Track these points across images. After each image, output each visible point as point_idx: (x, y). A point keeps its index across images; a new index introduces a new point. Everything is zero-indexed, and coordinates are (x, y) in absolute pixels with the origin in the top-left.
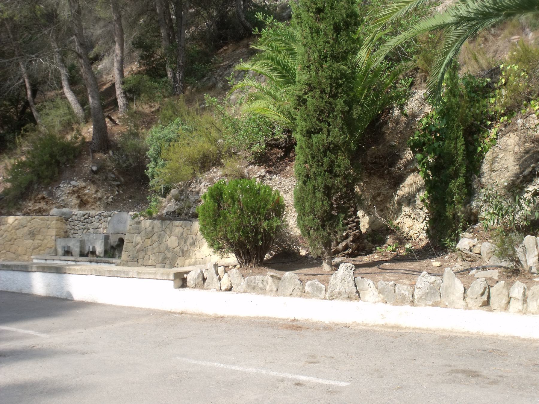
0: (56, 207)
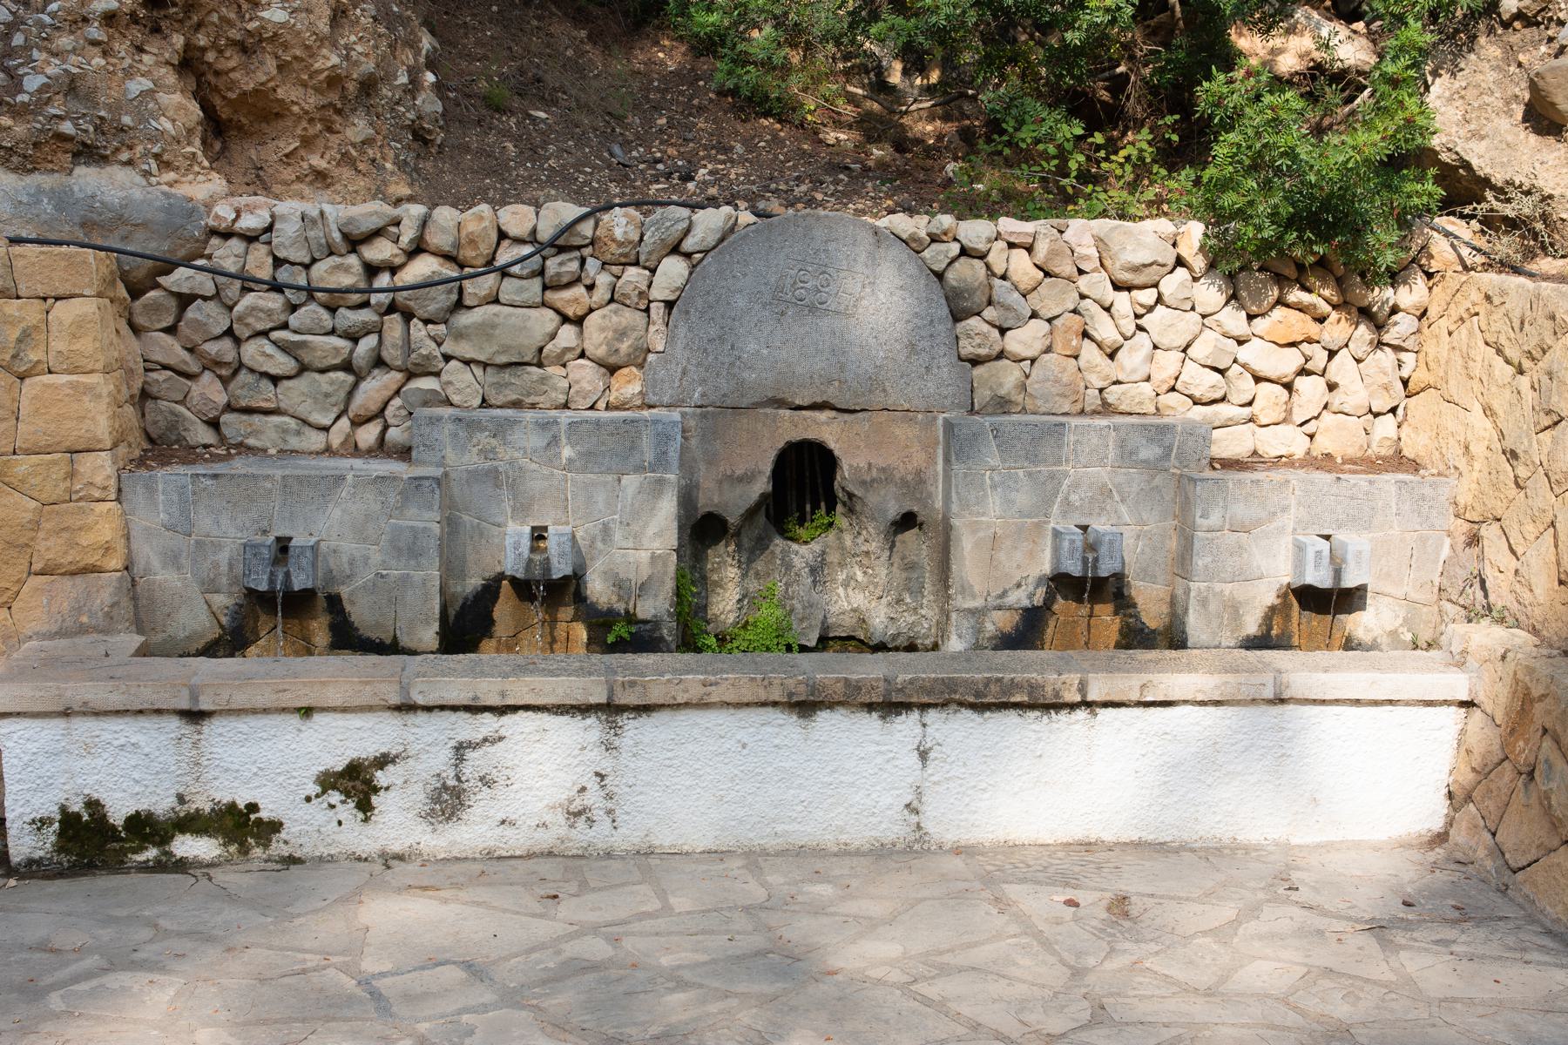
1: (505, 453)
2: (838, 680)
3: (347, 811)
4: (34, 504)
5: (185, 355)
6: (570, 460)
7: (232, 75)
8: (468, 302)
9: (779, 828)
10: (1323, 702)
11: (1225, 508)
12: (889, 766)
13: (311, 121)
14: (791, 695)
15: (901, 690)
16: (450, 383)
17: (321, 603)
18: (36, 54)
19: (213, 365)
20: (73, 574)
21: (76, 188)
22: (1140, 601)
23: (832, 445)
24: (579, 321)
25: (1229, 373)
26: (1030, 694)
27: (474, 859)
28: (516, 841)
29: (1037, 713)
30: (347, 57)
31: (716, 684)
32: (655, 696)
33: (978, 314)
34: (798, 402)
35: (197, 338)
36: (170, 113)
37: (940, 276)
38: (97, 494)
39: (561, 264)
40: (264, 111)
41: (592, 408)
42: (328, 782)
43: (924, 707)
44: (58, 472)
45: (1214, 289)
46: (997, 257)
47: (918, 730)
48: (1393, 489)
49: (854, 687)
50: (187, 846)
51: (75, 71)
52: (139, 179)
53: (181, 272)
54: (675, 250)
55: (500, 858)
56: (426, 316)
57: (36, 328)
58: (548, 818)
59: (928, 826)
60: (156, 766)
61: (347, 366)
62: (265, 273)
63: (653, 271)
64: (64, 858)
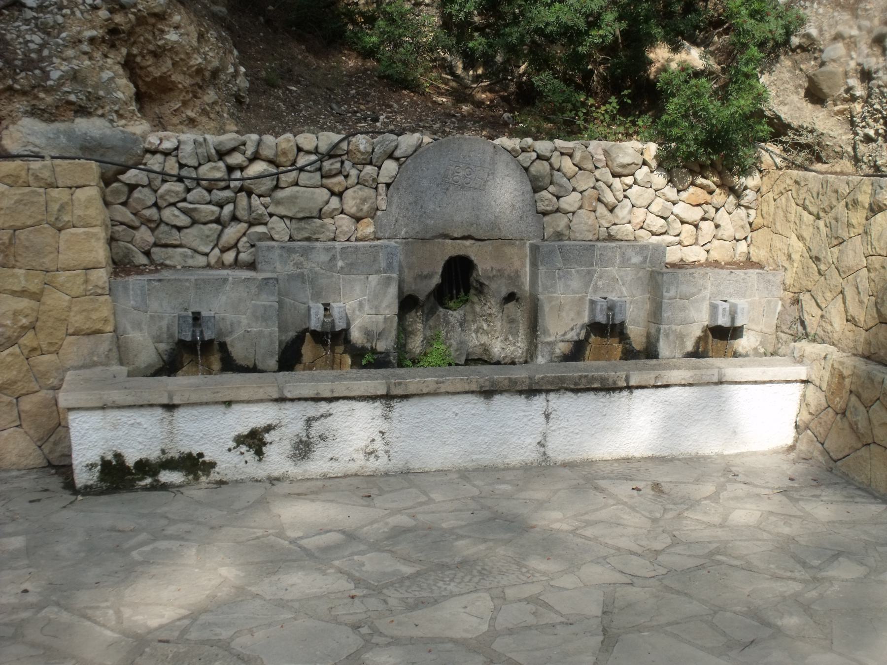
0: (34, 112)
1: (308, 265)
2: (505, 379)
3: (250, 455)
4: (68, 298)
5: (132, 216)
6: (342, 268)
7: (149, 69)
8: (282, 185)
9: (474, 457)
10: (740, 383)
11: (677, 287)
12: (529, 423)
13: (187, 92)
14: (481, 387)
15: (537, 383)
16: (273, 228)
17: (216, 347)
18: (55, 60)
19: (147, 221)
20: (88, 334)
21: (77, 130)
22: (631, 335)
23: (473, 258)
24: (340, 195)
25: (669, 219)
26: (601, 383)
27: (317, 479)
28: (336, 469)
29: (604, 393)
30: (205, 59)
31: (443, 382)
32: (412, 389)
33: (546, 189)
34: (455, 235)
35: (139, 208)
36: (122, 89)
37: (526, 169)
38: (100, 291)
39: (332, 164)
40: (164, 87)
41: (348, 240)
42: (240, 440)
43: (548, 391)
44: (80, 280)
45: (661, 177)
46: (555, 160)
47: (545, 403)
48: (756, 277)
49: (513, 382)
50: (166, 476)
51: (77, 68)
52: (107, 124)
53: (133, 172)
54: (391, 156)
55: (330, 478)
56: (260, 193)
57: (67, 203)
58: (355, 456)
59: (550, 453)
60: (150, 435)
61: (217, 221)
62: (175, 171)
63: (379, 168)
64: (104, 485)
